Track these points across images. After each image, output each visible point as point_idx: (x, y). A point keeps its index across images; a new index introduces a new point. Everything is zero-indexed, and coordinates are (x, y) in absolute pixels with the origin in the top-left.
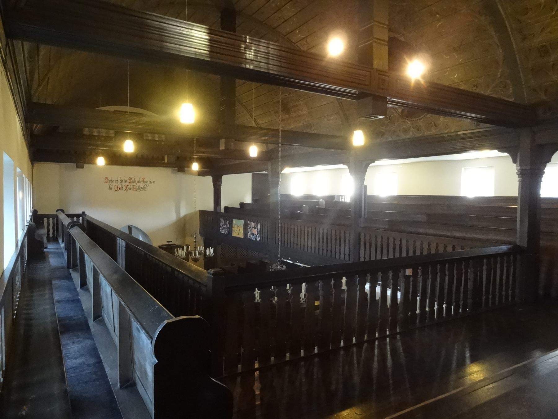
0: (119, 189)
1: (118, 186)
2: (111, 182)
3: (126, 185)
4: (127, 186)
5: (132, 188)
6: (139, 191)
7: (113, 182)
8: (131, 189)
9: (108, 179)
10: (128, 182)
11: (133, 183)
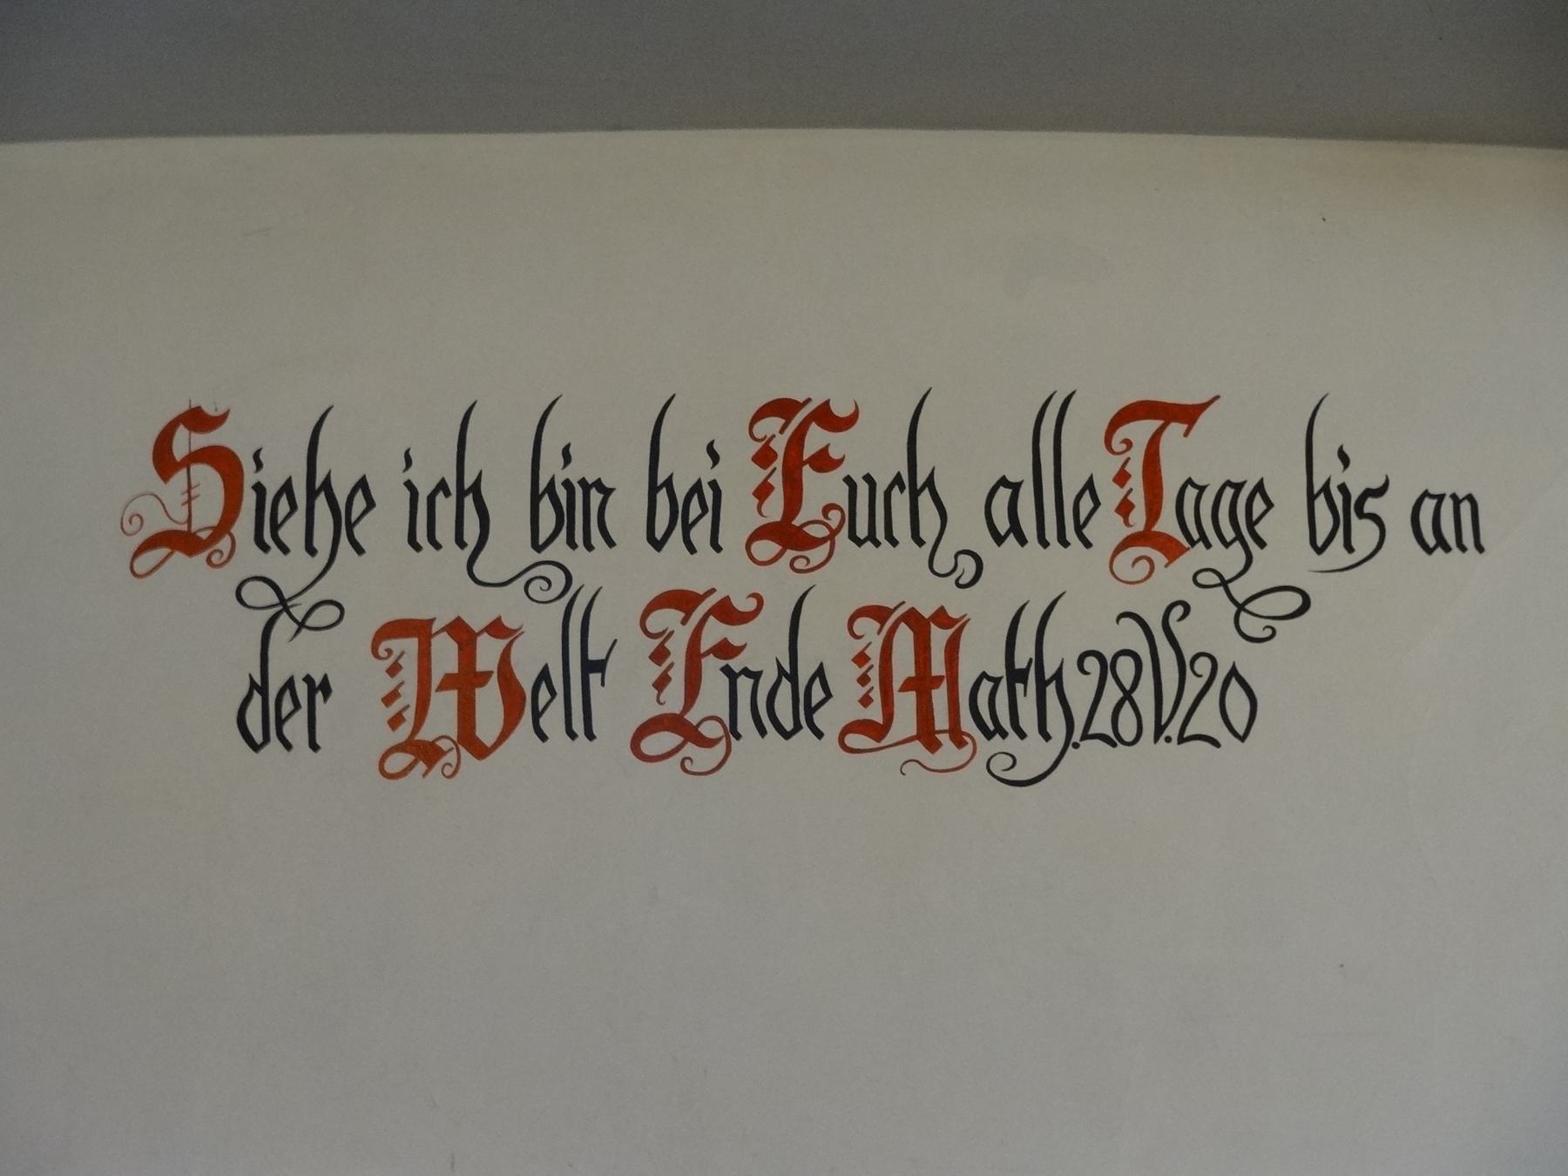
0: (489, 702)
1: (460, 631)
2: (292, 531)
3: (683, 601)
4: (715, 632)
5: (843, 678)
6: (1033, 754)
7: (344, 524)
8: (807, 712)
9: (223, 460)
10: (740, 516)
11: (878, 535)
